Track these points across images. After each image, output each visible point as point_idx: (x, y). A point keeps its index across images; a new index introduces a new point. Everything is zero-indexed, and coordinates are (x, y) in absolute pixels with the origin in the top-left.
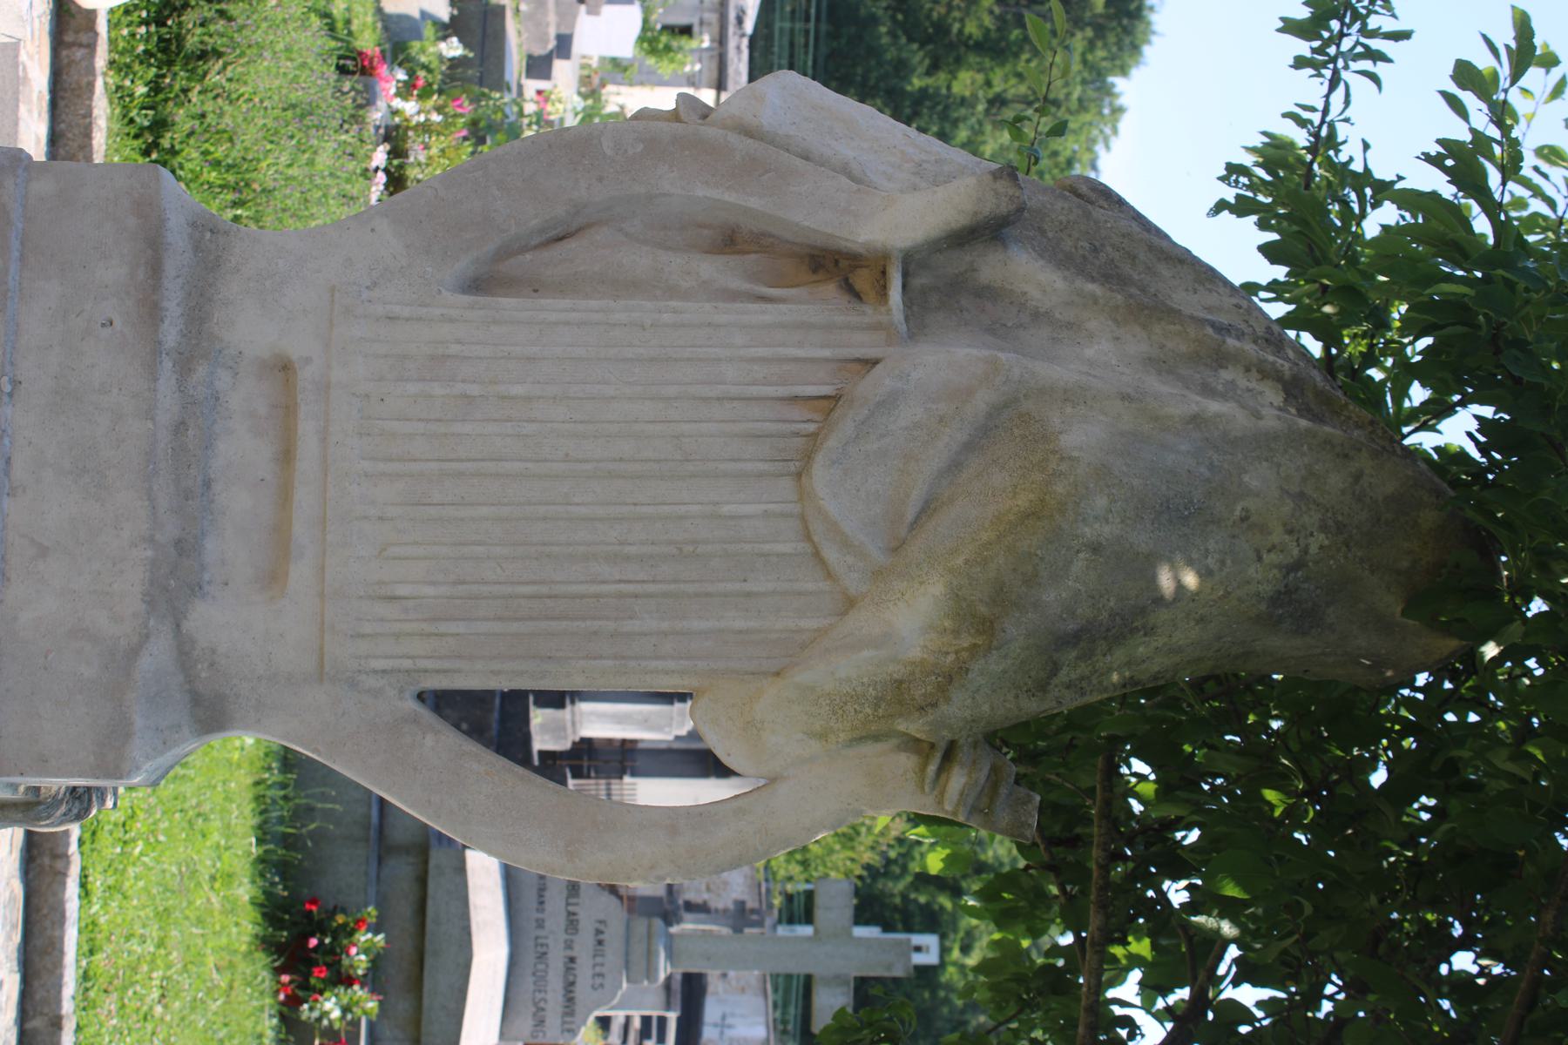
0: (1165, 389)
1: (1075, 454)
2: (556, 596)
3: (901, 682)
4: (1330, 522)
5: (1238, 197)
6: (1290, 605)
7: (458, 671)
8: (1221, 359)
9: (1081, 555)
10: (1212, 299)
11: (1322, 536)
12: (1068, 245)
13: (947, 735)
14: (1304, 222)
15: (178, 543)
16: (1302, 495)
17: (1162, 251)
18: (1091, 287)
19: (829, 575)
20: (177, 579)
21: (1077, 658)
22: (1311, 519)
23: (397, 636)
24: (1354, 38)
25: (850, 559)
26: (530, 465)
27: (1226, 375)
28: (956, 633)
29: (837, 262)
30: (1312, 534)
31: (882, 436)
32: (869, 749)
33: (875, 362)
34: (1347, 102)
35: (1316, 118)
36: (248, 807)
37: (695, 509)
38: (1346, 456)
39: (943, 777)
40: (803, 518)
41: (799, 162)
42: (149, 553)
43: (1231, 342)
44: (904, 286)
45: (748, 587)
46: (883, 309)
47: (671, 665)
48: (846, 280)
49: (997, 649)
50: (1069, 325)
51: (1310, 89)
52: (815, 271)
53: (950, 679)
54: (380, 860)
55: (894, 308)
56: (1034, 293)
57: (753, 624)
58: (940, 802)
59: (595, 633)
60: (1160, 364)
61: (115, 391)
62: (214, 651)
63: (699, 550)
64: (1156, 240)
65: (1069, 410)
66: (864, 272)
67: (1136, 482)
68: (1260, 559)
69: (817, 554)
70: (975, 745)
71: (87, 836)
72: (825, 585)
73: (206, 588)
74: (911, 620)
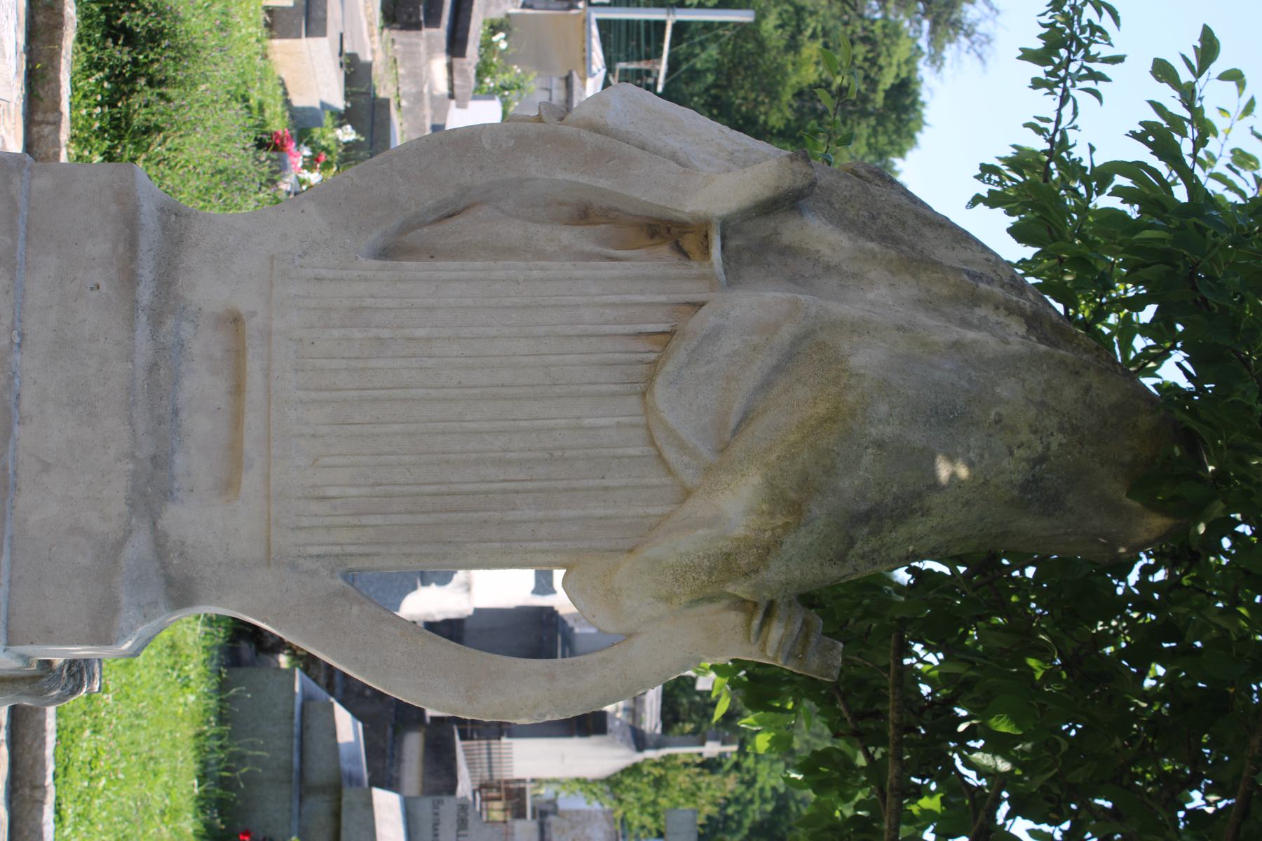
0: (933, 323)
1: (862, 371)
2: (454, 494)
3: (729, 554)
4: (1067, 425)
5: (990, 192)
6: (1038, 492)
7: (378, 554)
8: (975, 300)
9: (869, 451)
10: (967, 255)
11: (1060, 436)
12: (851, 214)
13: (767, 595)
14: (1044, 210)
15: (153, 458)
16: (1043, 404)
17: (926, 218)
18: (870, 245)
19: (669, 471)
20: (153, 487)
21: (870, 533)
22: (1051, 422)
23: (328, 528)
24: (1079, 63)
25: (686, 459)
26: (430, 391)
27: (980, 312)
28: (772, 514)
29: (669, 230)
30: (1052, 434)
31: (709, 362)
32: (706, 608)
33: (701, 305)
34: (1075, 113)
35: (1051, 127)
36: (191, 754)
37: (563, 422)
38: (1077, 373)
39: (765, 629)
40: (648, 428)
41: (637, 151)
42: (131, 466)
43: (983, 286)
44: (723, 247)
45: (606, 482)
46: (706, 264)
47: (546, 545)
48: (677, 243)
49: (805, 525)
50: (854, 276)
51: (1045, 104)
53: (768, 550)
54: (301, 799)
55: (716, 265)
56: (825, 250)
57: (610, 512)
58: (763, 650)
59: (485, 522)
60: (928, 304)
61: (102, 339)
62: (183, 543)
63: (568, 454)
64: (921, 210)
65: (856, 339)
66: (691, 237)
67: (910, 392)
68: (1011, 454)
69: (660, 456)
70: (790, 604)
71: (60, 770)
72: (666, 480)
73: (176, 494)
74: (736, 505)
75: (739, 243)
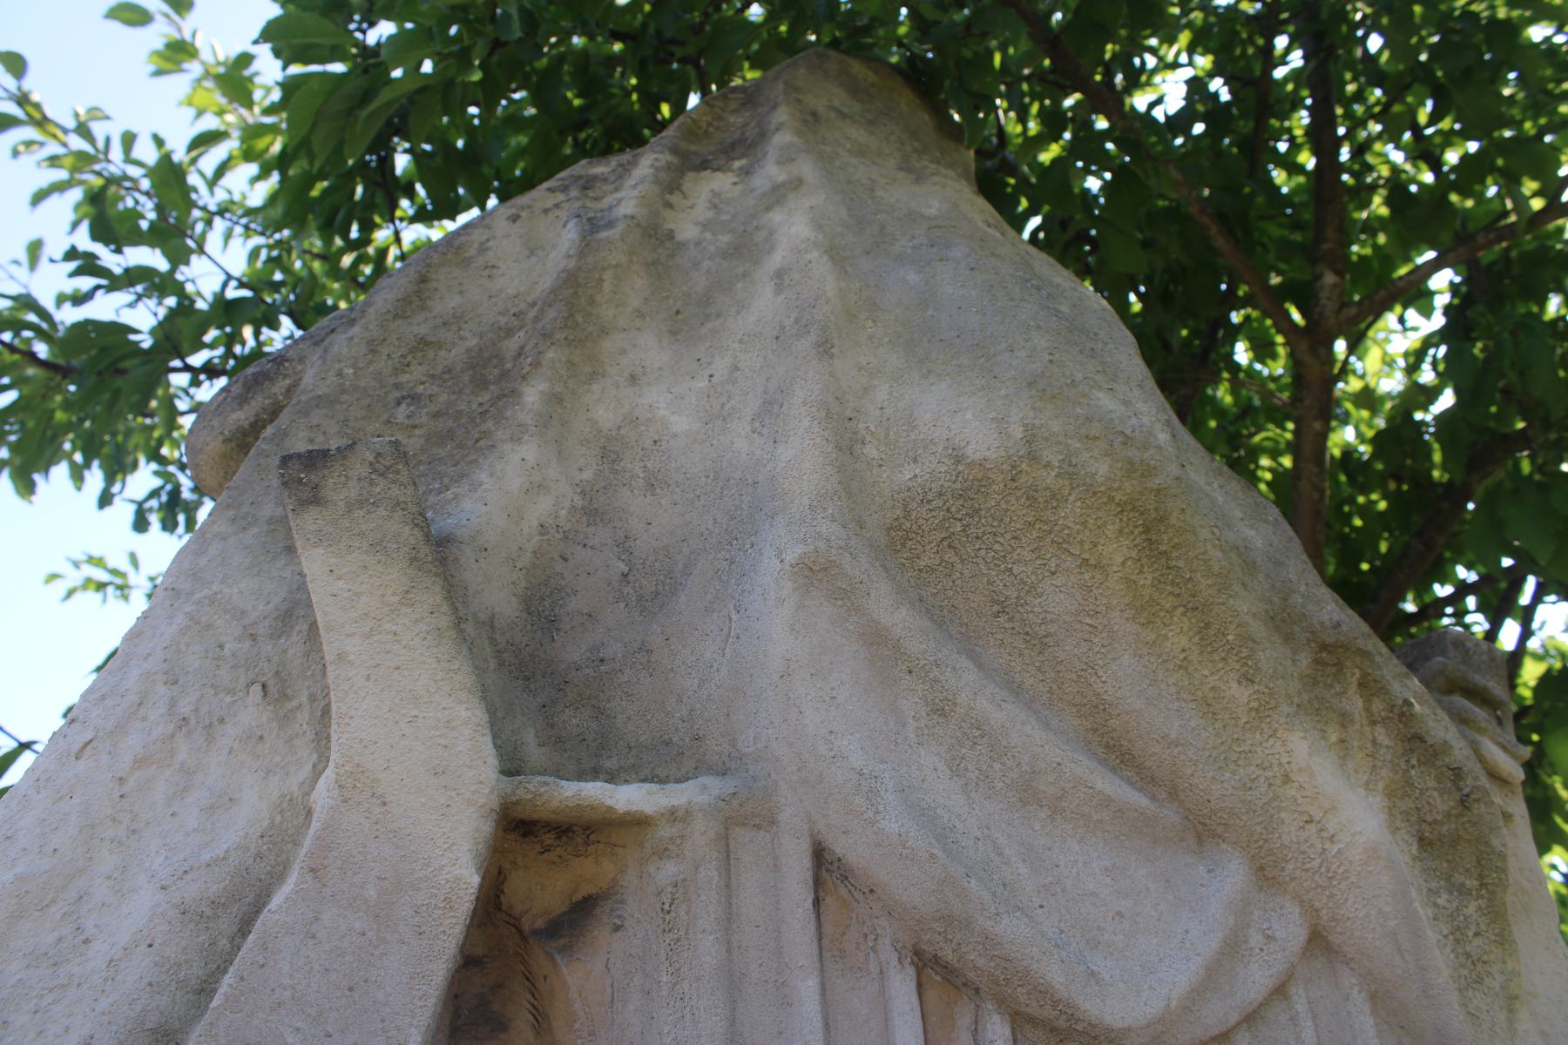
1: (1018, 432)
3: (1423, 842)
17: (405, 301)
18: (533, 394)
25: (1255, 939)
33: (820, 855)
46: (665, 831)
52: (501, 1025)
56: (540, 509)
65: (871, 451)
75: (530, 737)
